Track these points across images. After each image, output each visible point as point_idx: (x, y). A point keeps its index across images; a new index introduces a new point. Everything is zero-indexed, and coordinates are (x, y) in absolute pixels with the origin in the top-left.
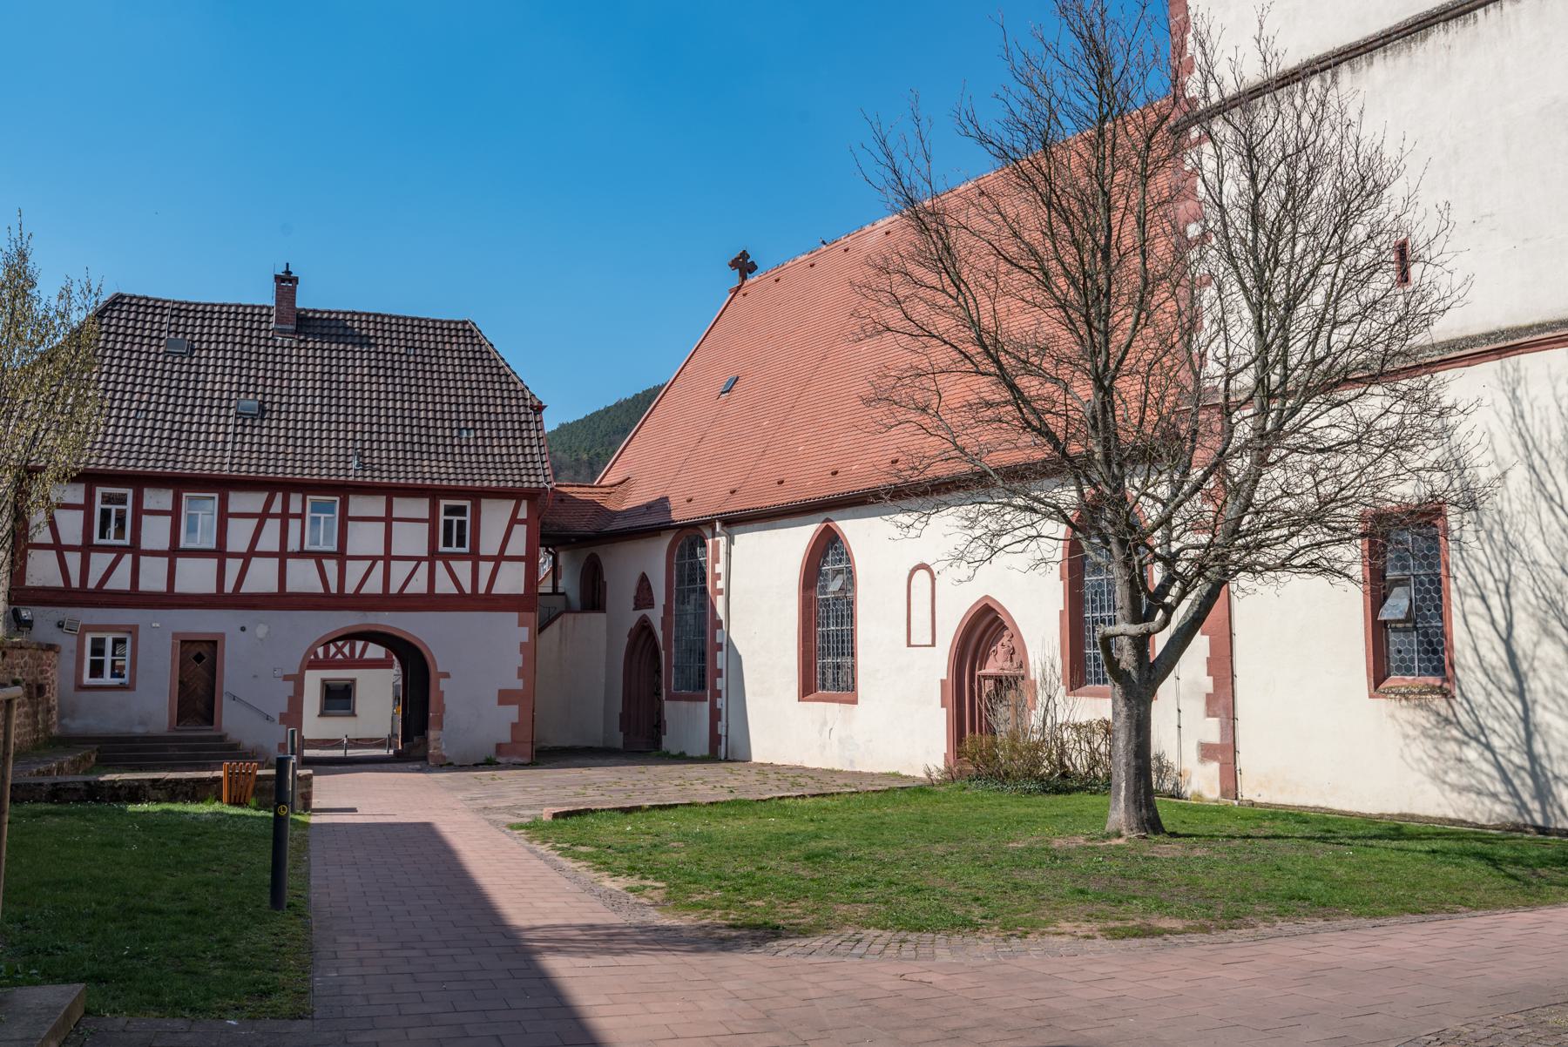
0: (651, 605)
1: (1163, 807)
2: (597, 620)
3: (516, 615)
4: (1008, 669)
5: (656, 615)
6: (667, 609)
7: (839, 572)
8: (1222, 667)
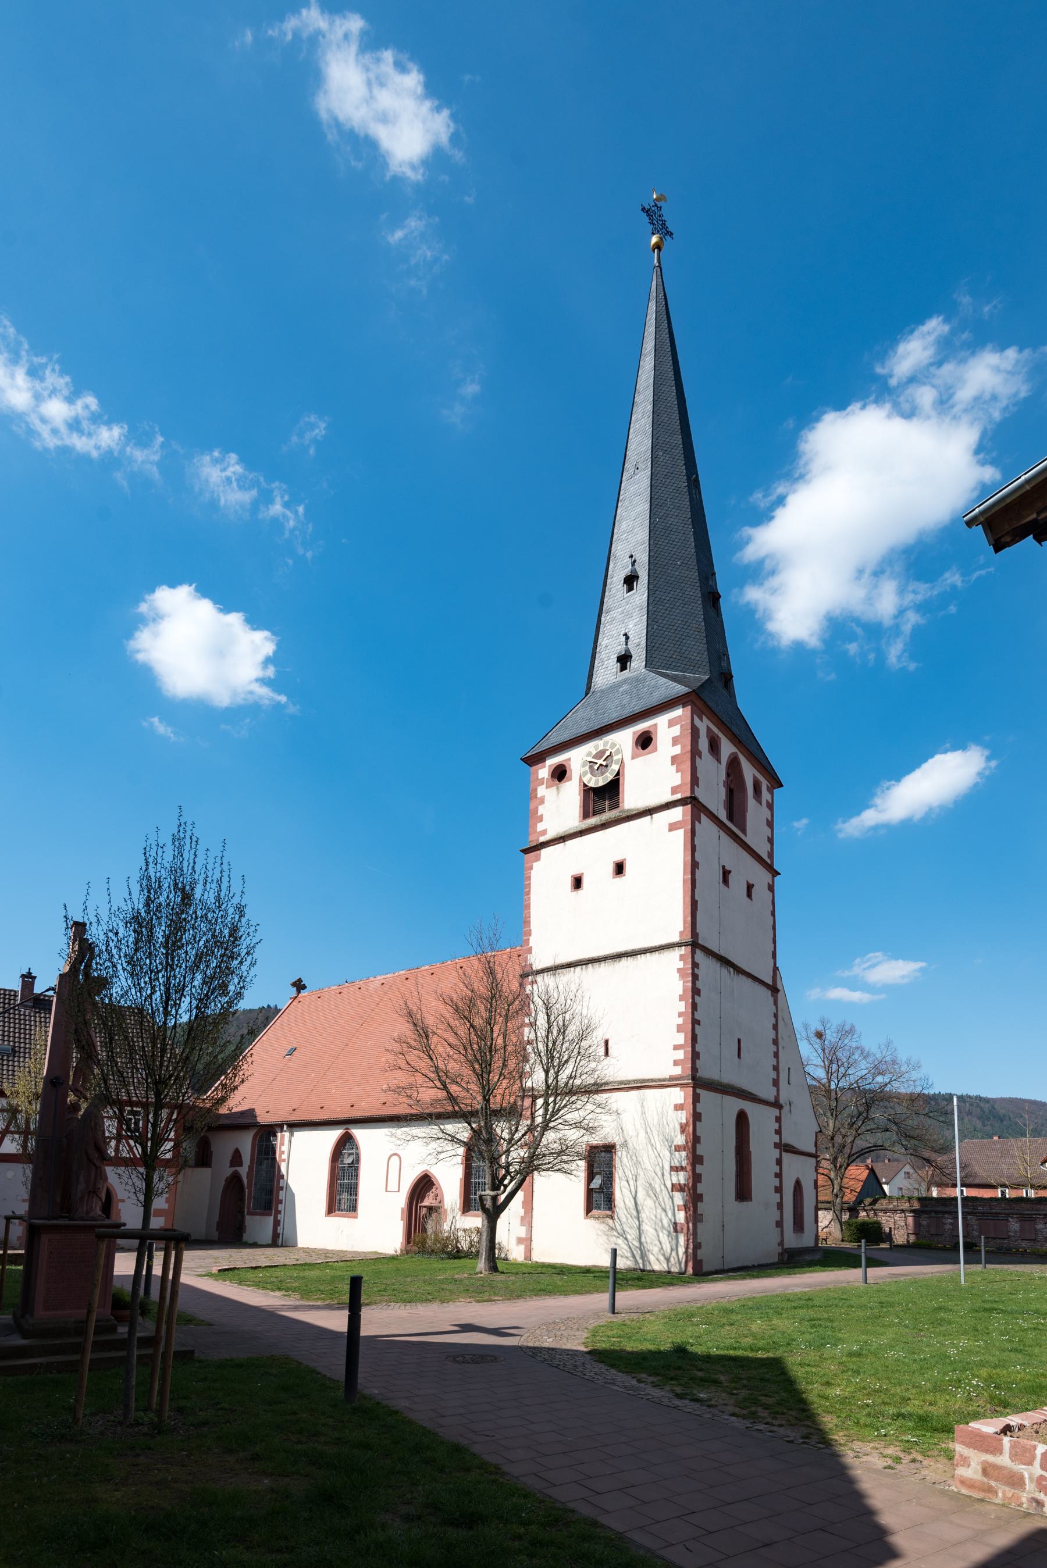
0: (241, 1164)
1: (500, 1265)
2: (205, 1173)
4: (435, 1204)
5: (243, 1171)
6: (250, 1167)
7: (350, 1154)
8: (528, 1205)
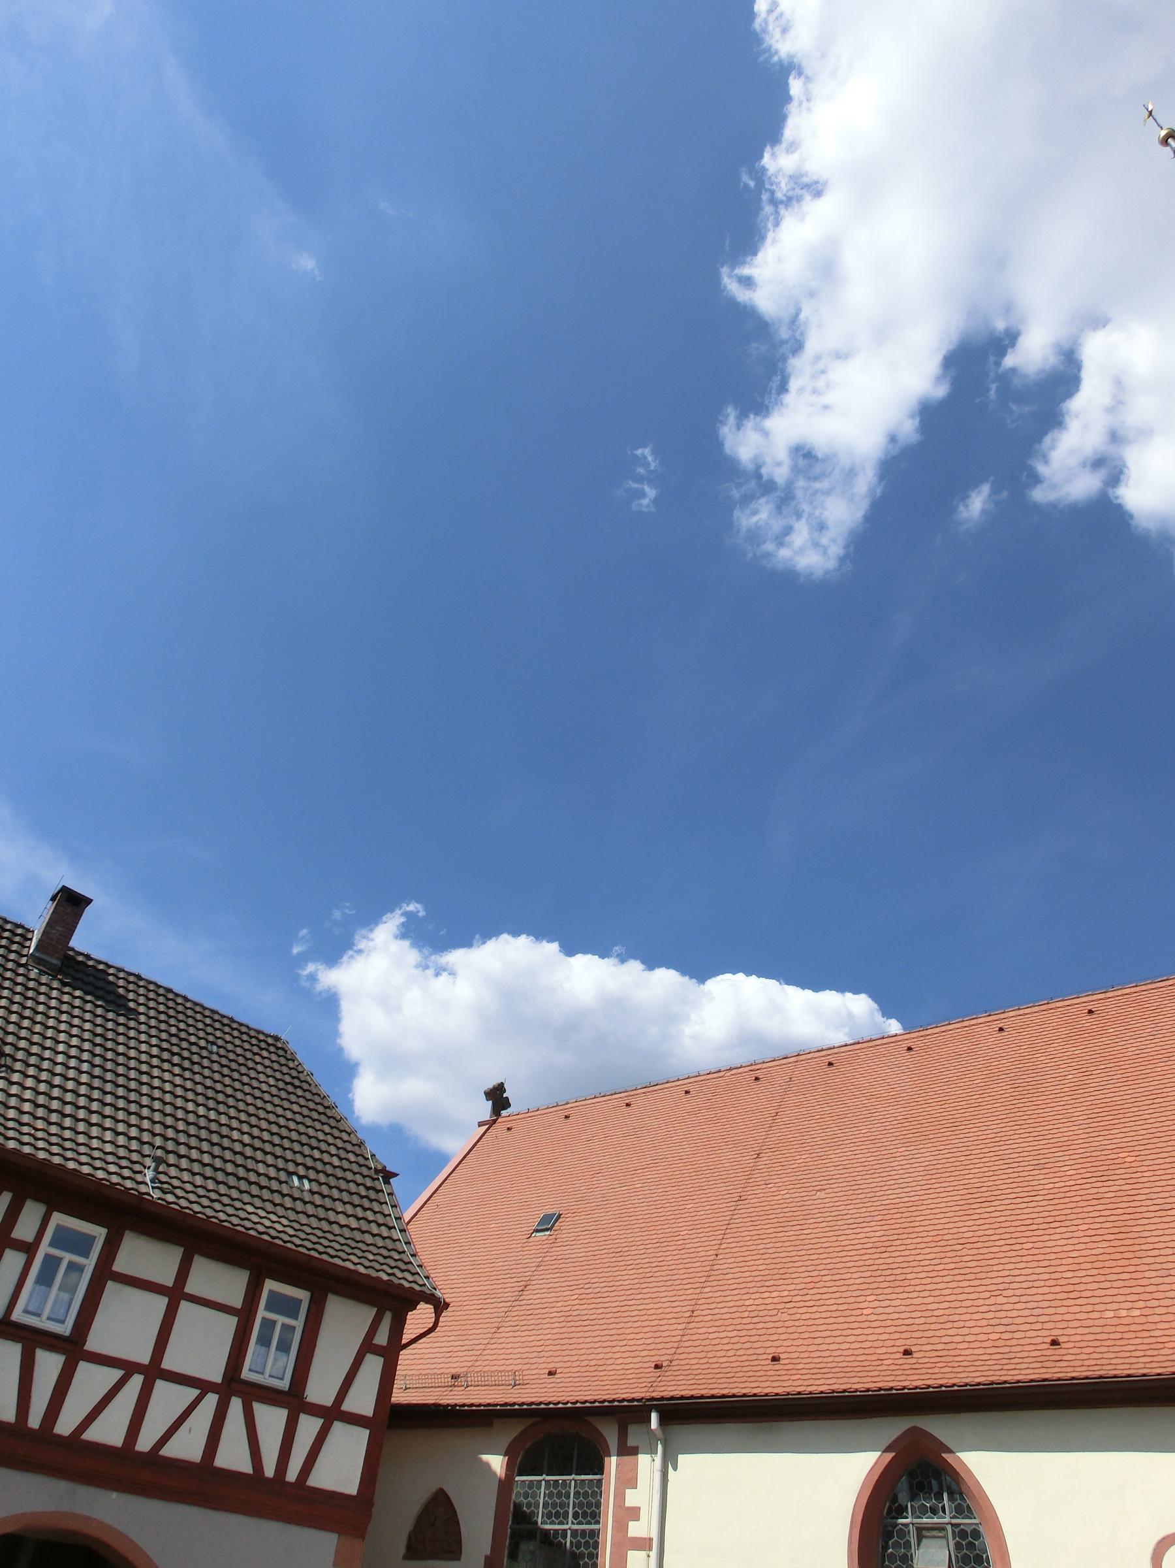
3: (334, 1537)
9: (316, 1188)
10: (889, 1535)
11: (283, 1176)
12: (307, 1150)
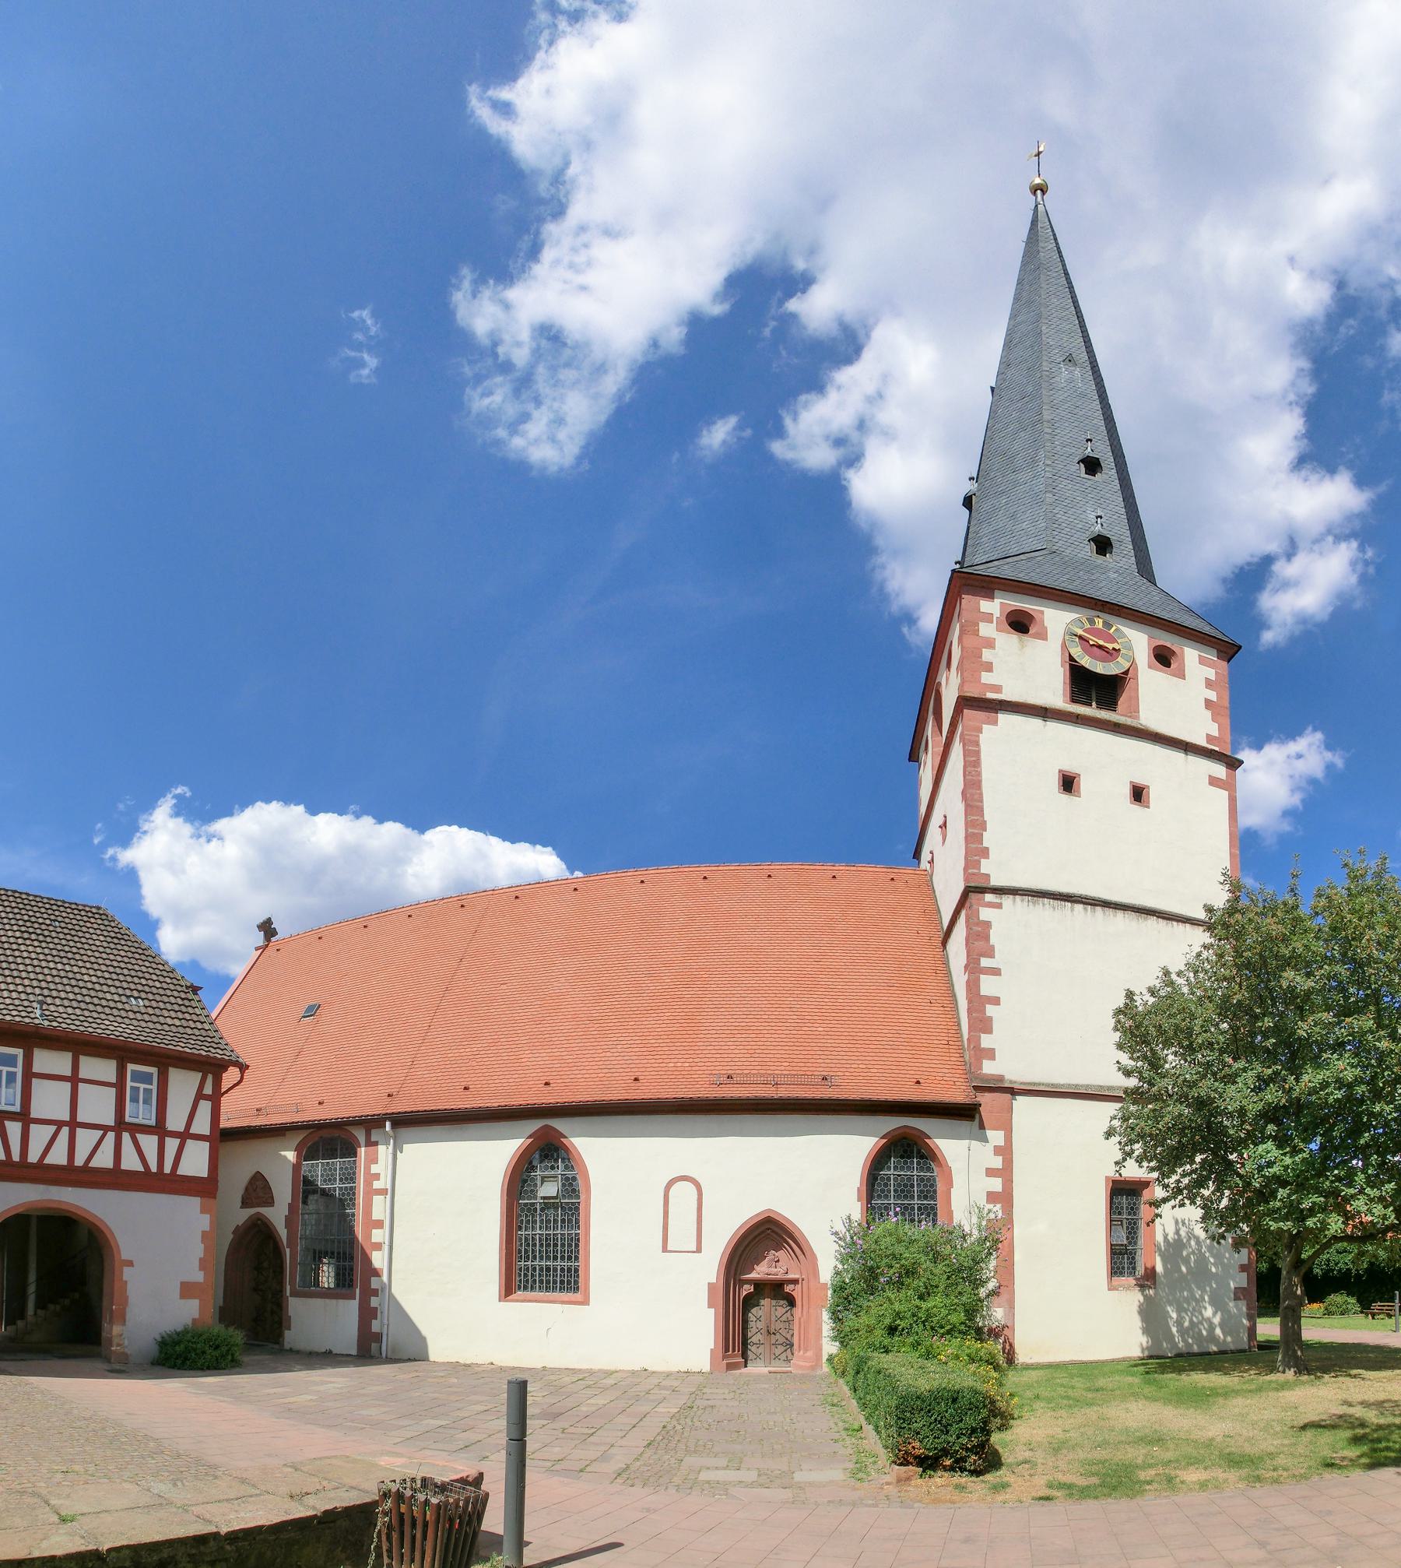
9: (147, 1003)
10: (525, 1181)
11: (124, 999)
12: (136, 980)
